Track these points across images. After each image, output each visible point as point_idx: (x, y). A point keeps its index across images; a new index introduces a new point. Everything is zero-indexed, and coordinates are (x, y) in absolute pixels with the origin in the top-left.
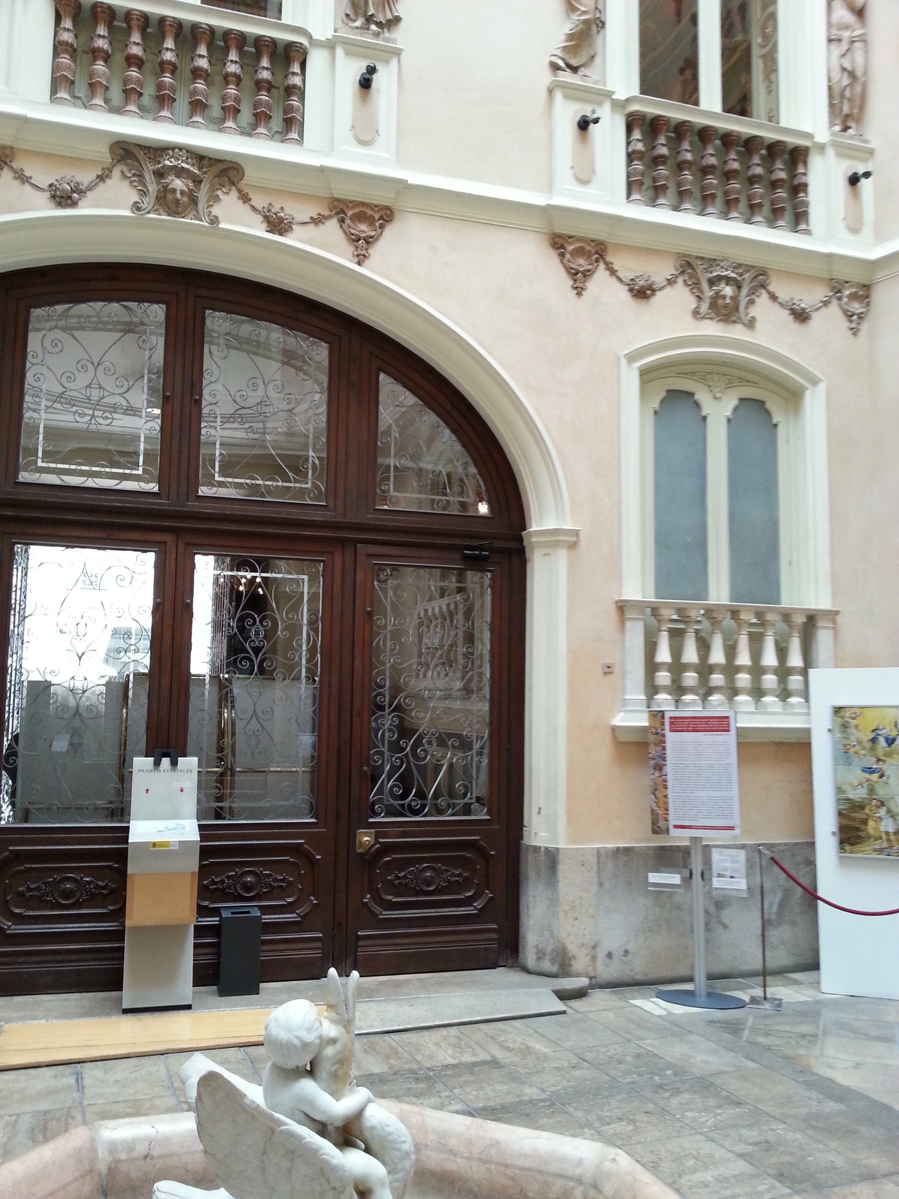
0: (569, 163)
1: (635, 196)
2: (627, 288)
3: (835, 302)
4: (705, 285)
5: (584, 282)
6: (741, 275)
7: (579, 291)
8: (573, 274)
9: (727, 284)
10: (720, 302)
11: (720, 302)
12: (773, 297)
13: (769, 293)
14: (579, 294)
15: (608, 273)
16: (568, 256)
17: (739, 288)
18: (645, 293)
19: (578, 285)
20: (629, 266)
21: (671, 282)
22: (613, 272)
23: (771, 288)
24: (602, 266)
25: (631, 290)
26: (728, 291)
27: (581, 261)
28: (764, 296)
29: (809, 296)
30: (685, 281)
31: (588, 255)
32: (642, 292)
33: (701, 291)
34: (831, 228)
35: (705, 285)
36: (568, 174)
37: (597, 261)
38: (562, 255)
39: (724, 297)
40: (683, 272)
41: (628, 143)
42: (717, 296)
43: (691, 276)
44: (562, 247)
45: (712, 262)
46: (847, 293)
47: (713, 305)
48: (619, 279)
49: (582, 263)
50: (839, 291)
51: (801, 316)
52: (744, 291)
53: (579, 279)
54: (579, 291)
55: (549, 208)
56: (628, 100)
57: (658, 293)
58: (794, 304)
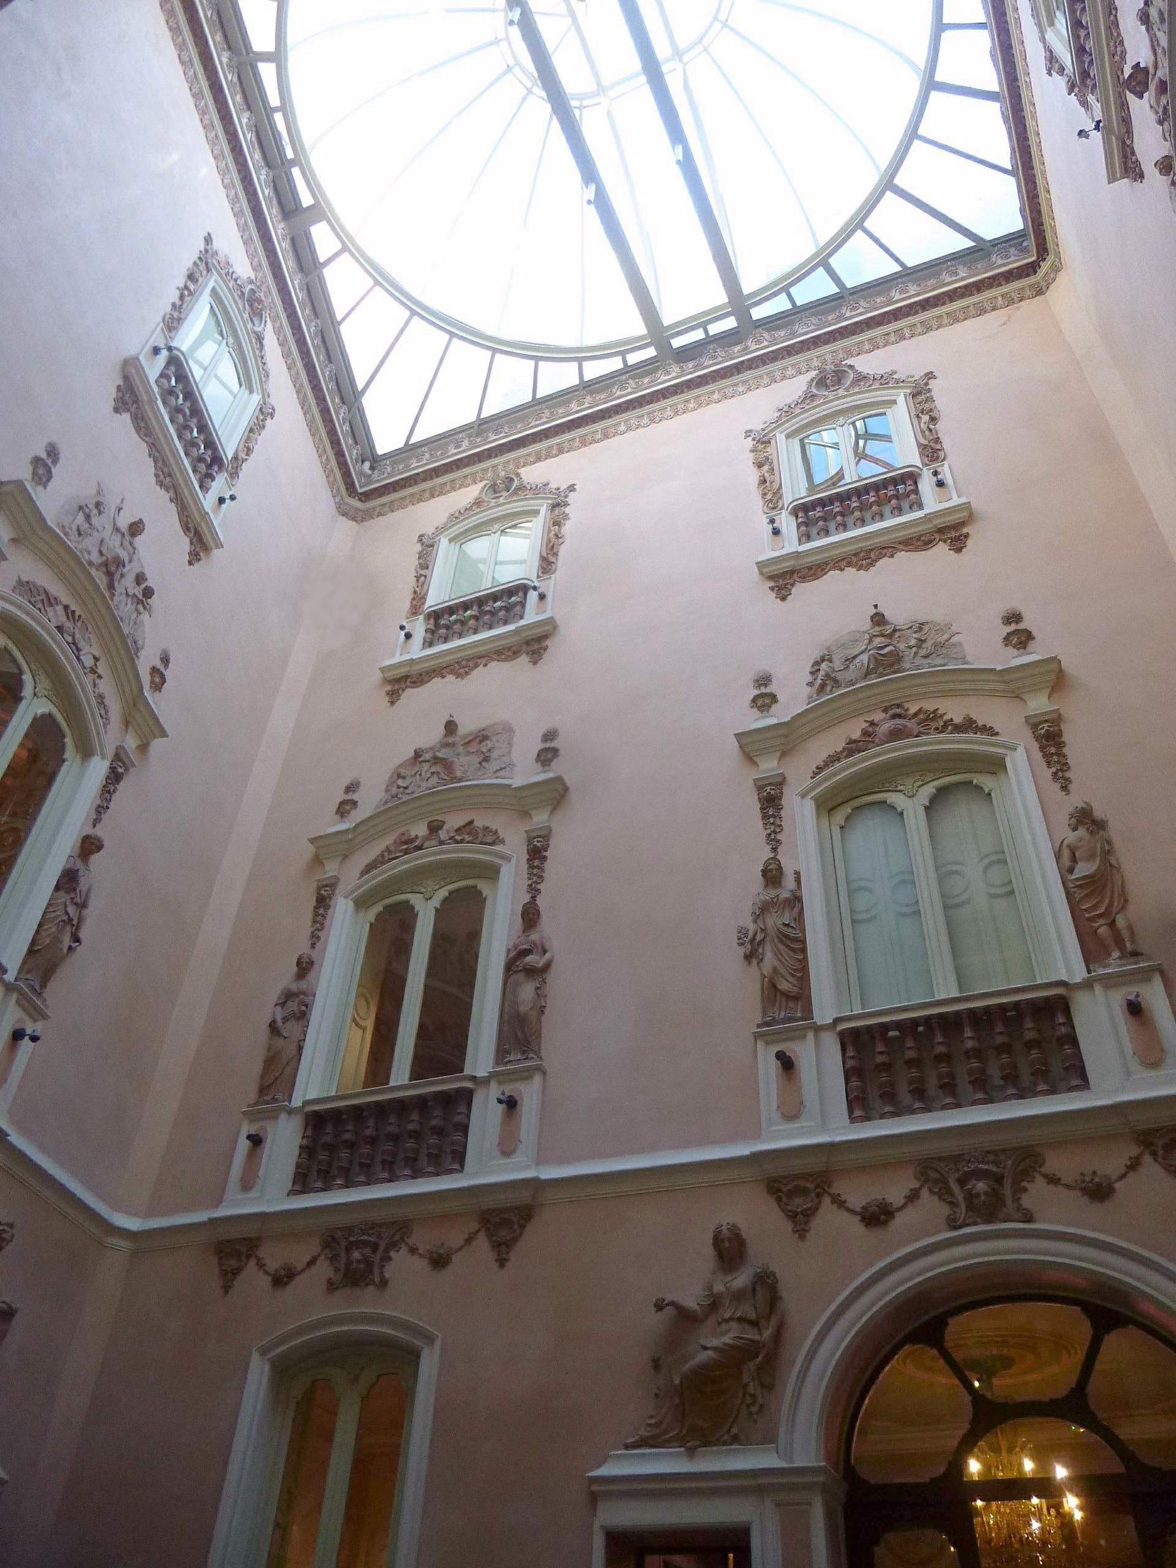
0: (774, 1104)
1: (858, 1113)
2: (859, 1218)
3: (1147, 1159)
4: (955, 1188)
5: (806, 1223)
6: (997, 1163)
7: (801, 1234)
8: (792, 1216)
9: (978, 1180)
10: (976, 1201)
11: (976, 1201)
12: (1053, 1180)
13: (1045, 1176)
14: (802, 1238)
15: (835, 1207)
16: (784, 1199)
17: (999, 1179)
18: (878, 1219)
19: (799, 1227)
20: (858, 1192)
21: (913, 1197)
22: (839, 1202)
23: (1047, 1168)
24: (827, 1200)
25: (863, 1219)
26: (981, 1186)
27: (798, 1201)
28: (1039, 1180)
29: (1108, 1162)
30: (930, 1190)
31: (803, 1191)
32: (877, 1216)
33: (953, 1195)
34: (1114, 1075)
35: (955, 1188)
36: (776, 1116)
37: (818, 1195)
38: (779, 1200)
39: (978, 1195)
40: (925, 1182)
41: (844, 1063)
42: (970, 1197)
43: (936, 1181)
44: (779, 1190)
45: (957, 1159)
46: (1161, 1143)
47: (970, 1206)
48: (849, 1210)
49: (799, 1203)
50: (1151, 1144)
51: (1099, 1192)
52: (1008, 1183)
53: (801, 1221)
54: (801, 1234)
55: (756, 1158)
56: (837, 1021)
57: (897, 1215)
58: (1083, 1181)
